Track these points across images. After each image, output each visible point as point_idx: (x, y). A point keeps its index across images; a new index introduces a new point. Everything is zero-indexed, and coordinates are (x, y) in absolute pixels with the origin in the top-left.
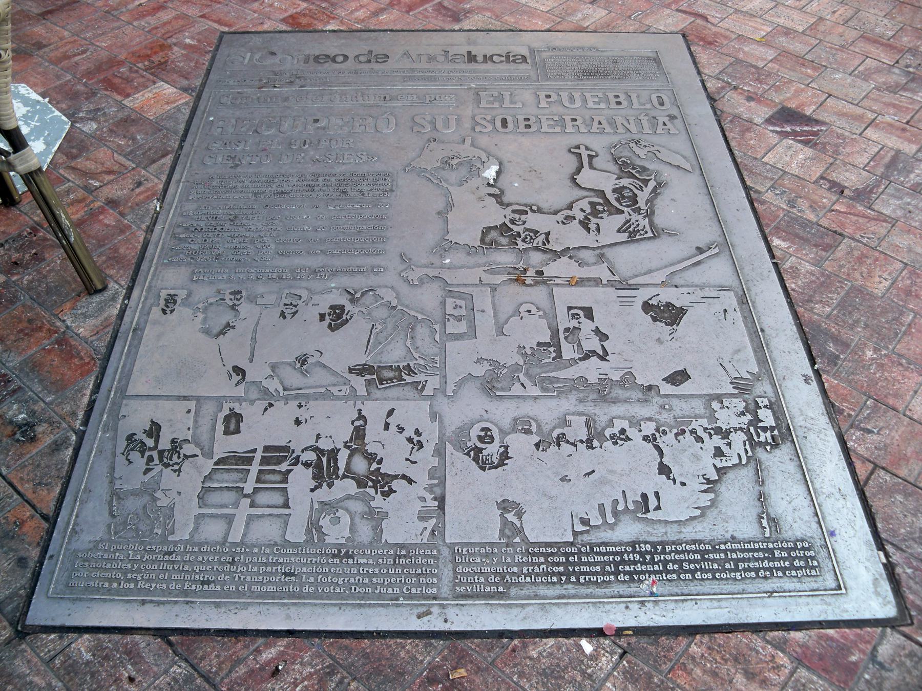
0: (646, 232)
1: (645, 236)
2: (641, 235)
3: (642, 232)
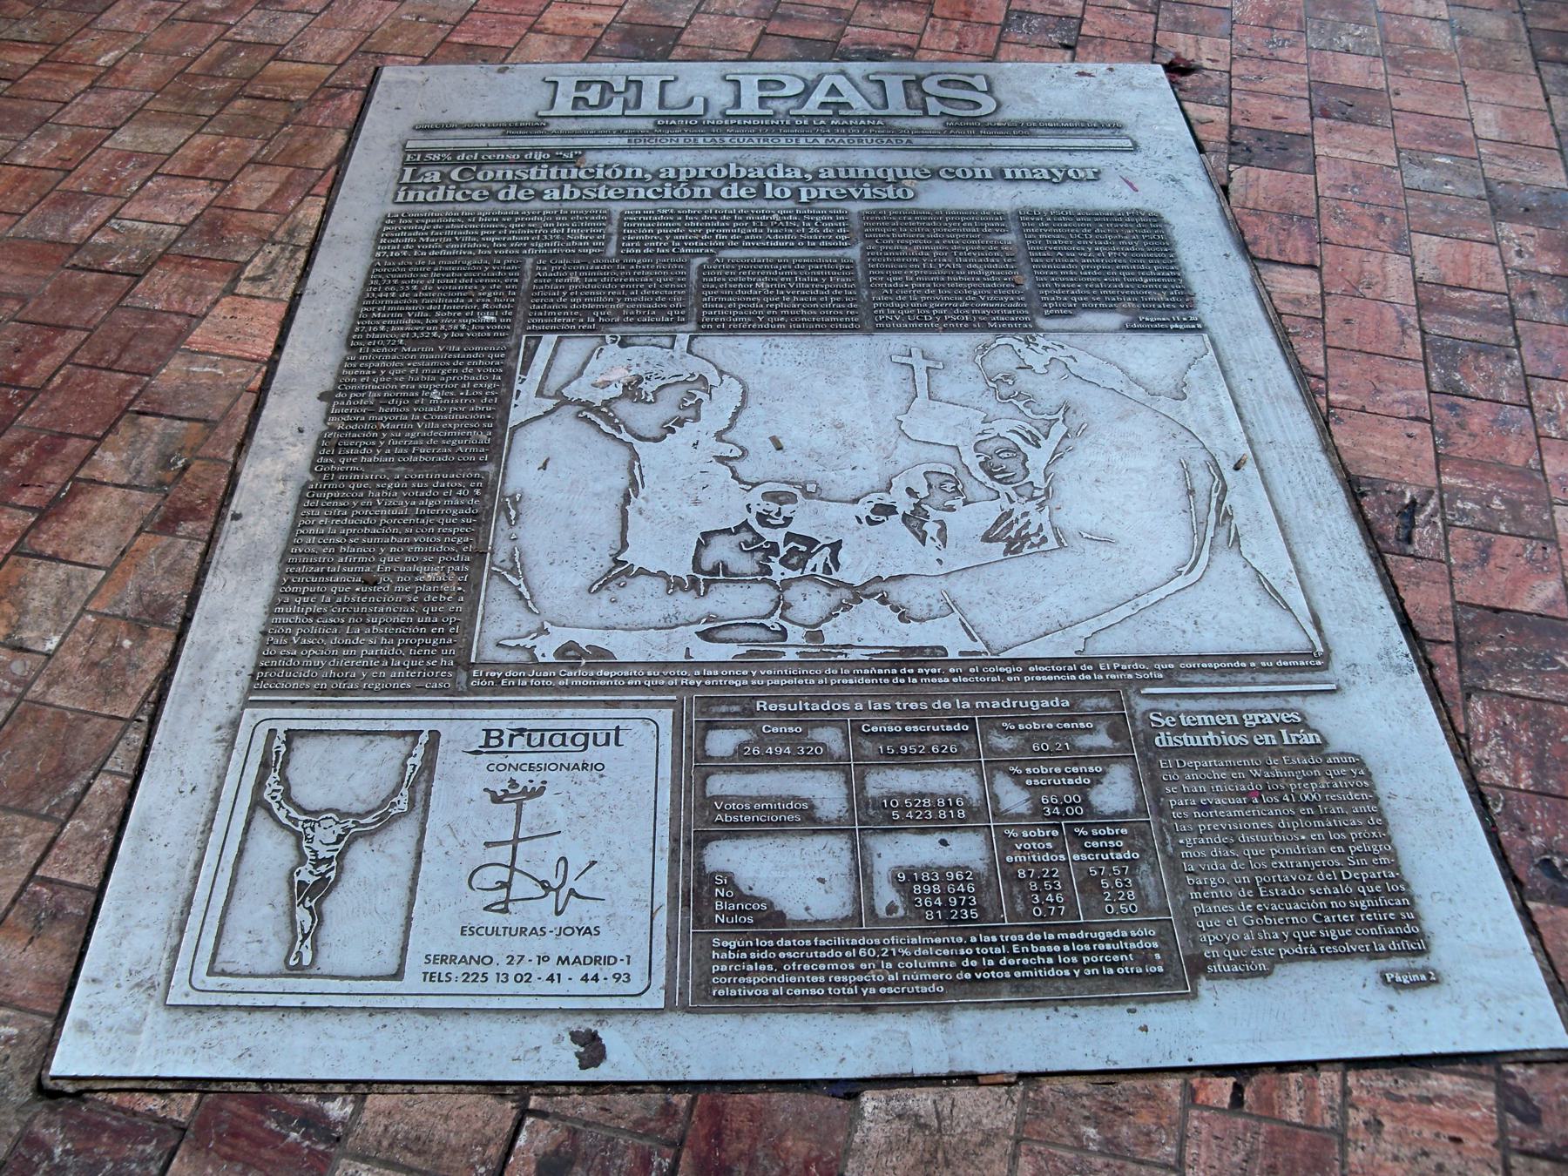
0: (1044, 540)
1: (1043, 547)
2: (1033, 545)
3: (1035, 540)
